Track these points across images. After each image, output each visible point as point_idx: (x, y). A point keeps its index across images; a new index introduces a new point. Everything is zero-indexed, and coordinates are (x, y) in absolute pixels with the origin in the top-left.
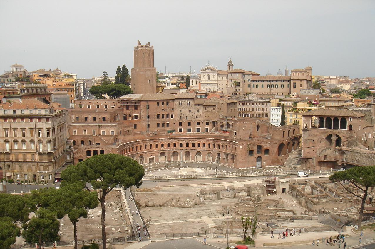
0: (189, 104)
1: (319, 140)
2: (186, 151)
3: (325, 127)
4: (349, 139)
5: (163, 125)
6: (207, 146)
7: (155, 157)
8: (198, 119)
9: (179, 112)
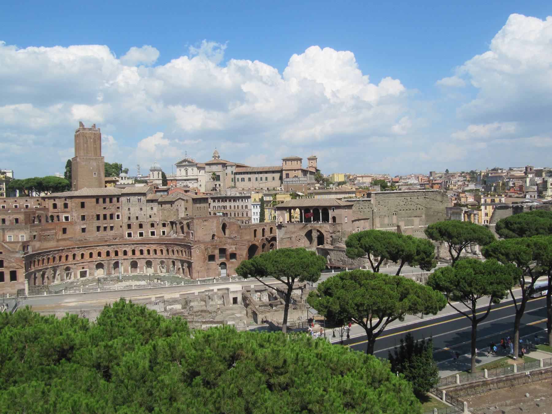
0: (140, 200)
1: (298, 238)
2: (132, 260)
4: (333, 235)
5: (105, 228)
6: (158, 252)
7: (88, 270)
8: (152, 219)
9: (127, 212)
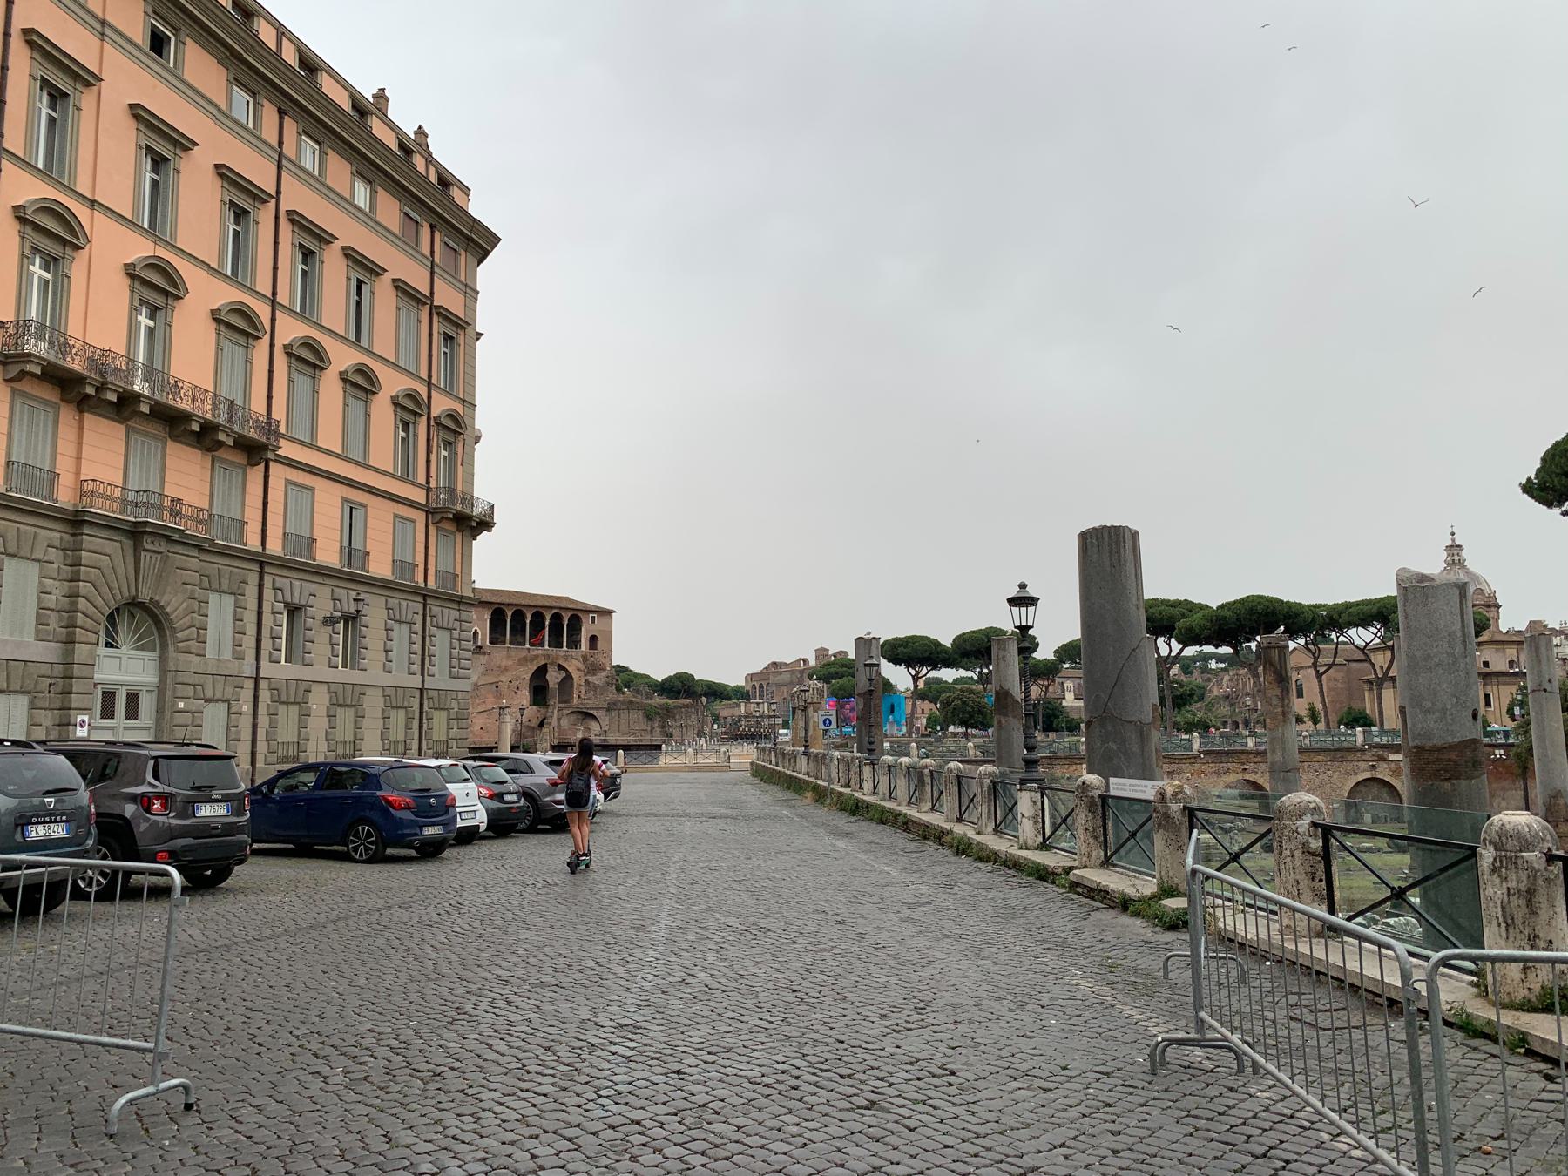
1: (515, 684)
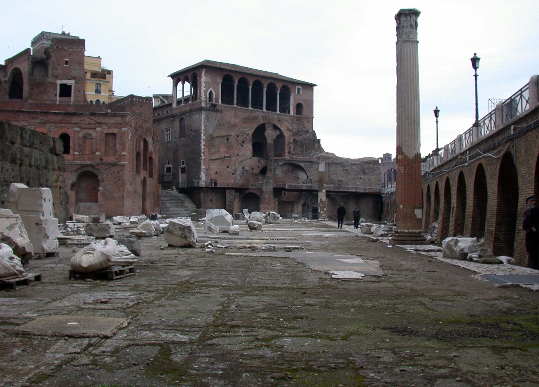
1: (241, 138)
3: (250, 105)
4: (298, 138)
